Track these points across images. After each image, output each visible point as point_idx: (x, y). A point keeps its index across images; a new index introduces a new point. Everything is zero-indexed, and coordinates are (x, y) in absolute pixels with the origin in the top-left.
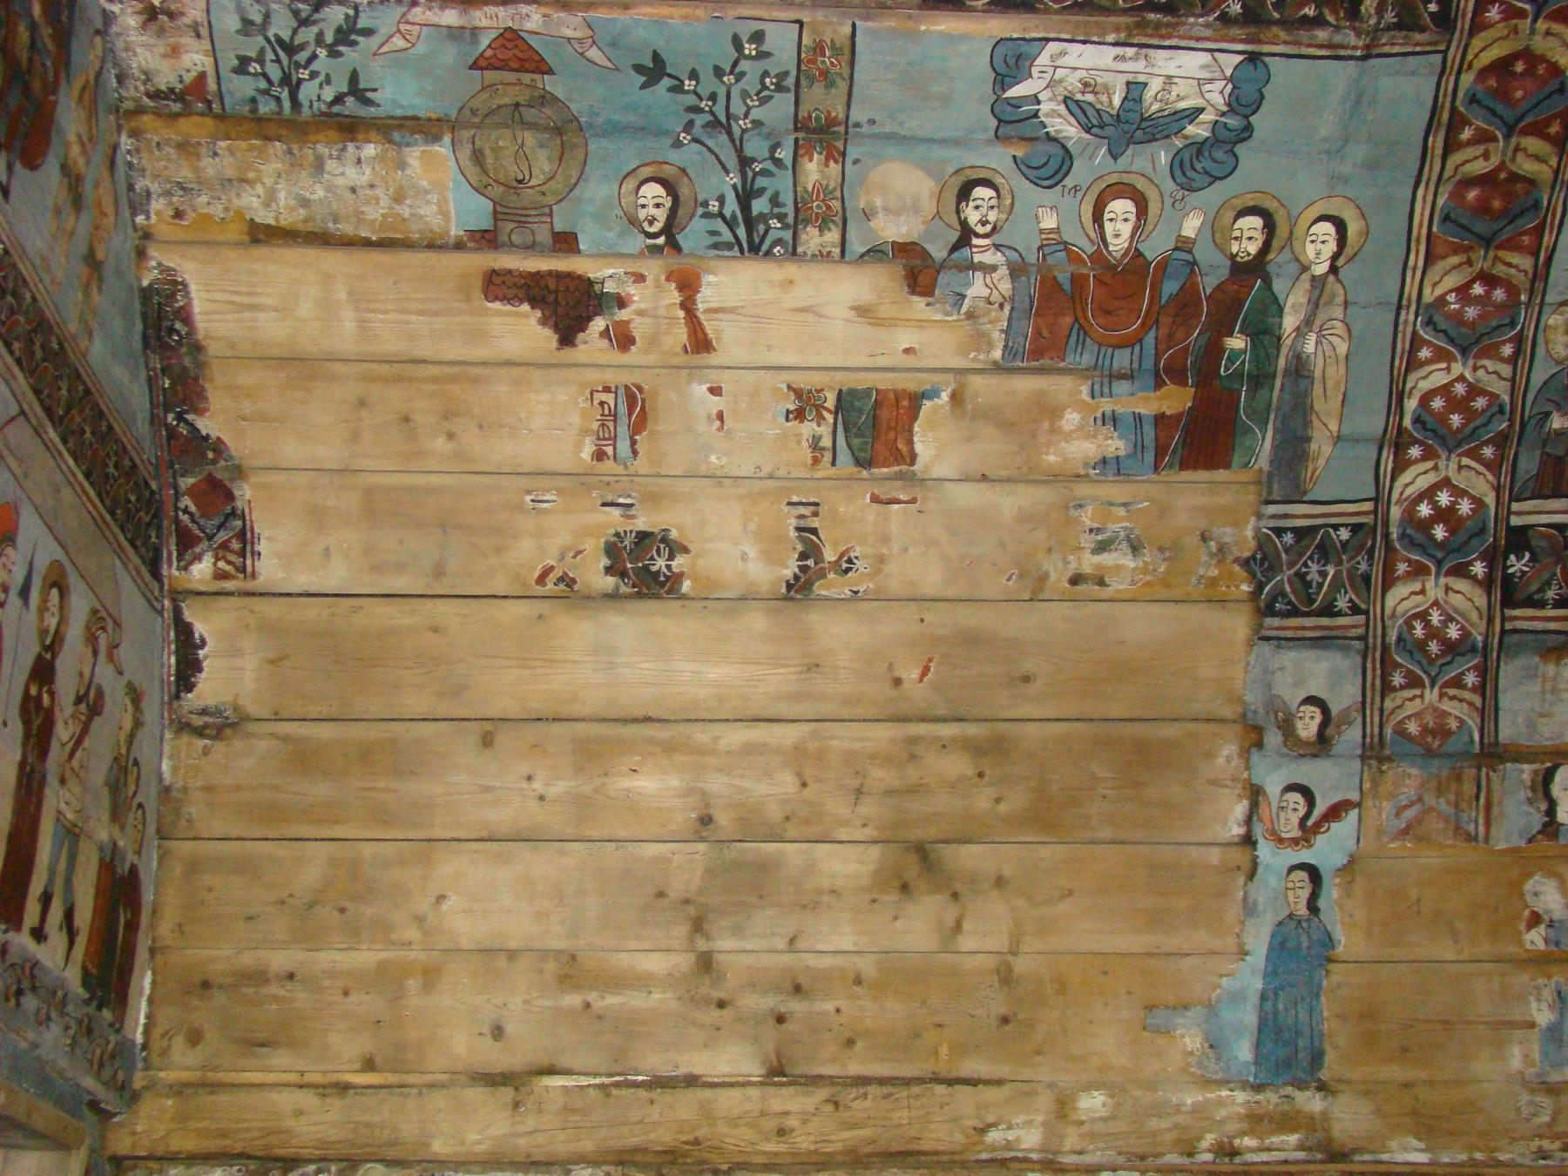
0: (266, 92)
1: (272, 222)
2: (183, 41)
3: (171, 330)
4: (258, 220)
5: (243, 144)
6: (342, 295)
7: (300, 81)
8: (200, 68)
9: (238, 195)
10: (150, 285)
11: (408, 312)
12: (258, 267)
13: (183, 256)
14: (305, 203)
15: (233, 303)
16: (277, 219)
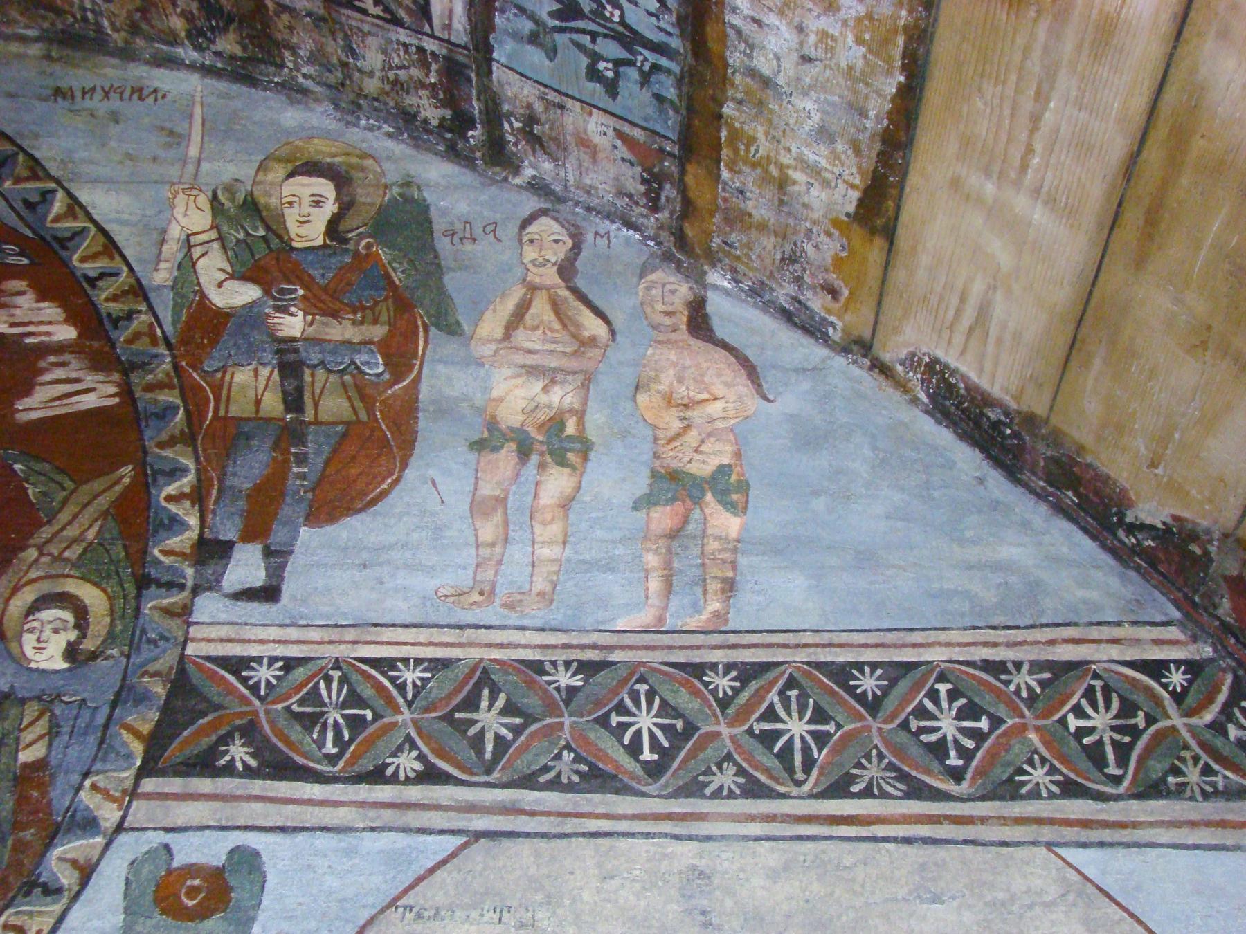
0: (645, 79)
1: (855, 195)
2: (570, 128)
3: (996, 425)
4: (851, 208)
5: (725, 153)
6: (990, 188)
7: (623, 22)
8: (610, 132)
9: (805, 205)
10: (928, 395)
11: (1036, 119)
12: (925, 260)
13: (897, 330)
14: (824, 134)
15: (971, 330)
16: (853, 186)
